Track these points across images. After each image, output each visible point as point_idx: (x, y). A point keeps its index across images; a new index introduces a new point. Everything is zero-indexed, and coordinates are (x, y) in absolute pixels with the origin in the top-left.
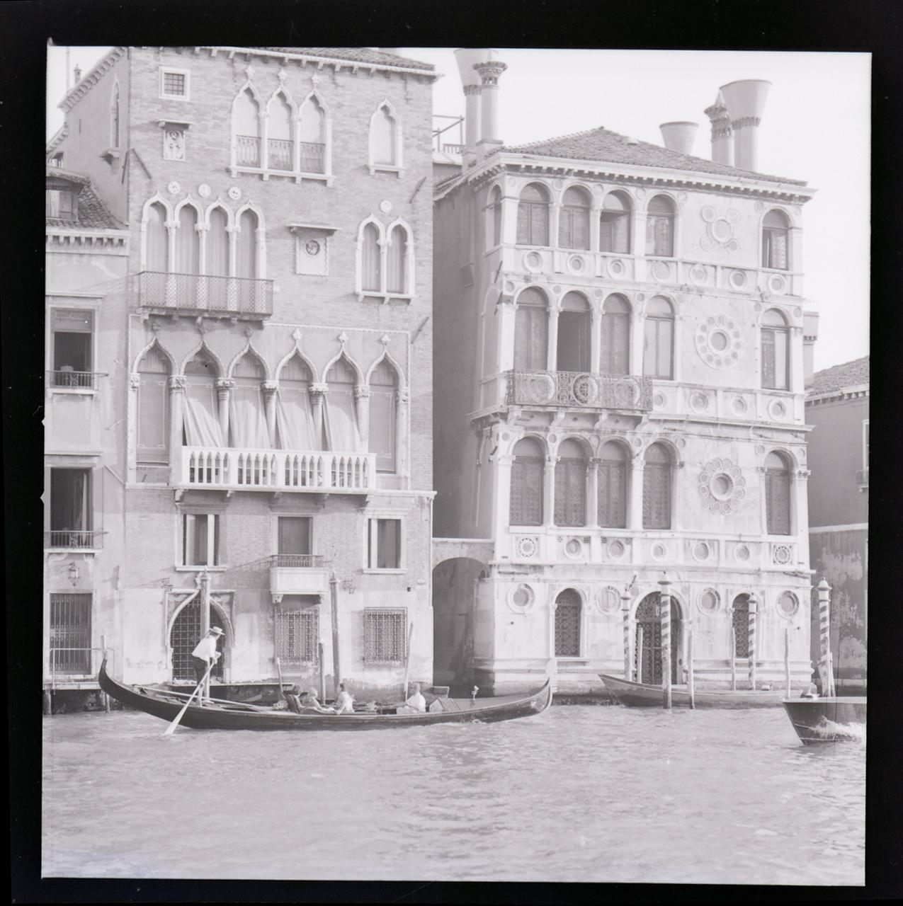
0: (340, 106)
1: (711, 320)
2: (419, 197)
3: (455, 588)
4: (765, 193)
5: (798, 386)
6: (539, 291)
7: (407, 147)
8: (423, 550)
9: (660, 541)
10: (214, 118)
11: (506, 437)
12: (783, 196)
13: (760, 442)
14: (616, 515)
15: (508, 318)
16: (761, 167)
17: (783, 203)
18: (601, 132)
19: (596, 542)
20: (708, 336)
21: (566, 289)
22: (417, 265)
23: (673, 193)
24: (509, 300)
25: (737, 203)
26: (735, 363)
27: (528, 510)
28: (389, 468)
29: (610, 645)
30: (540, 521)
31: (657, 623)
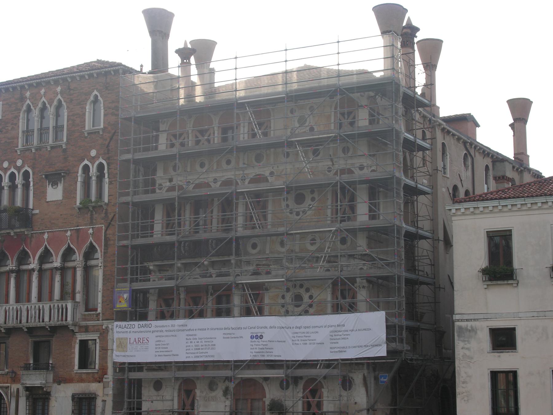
0: (71, 100)
7: (105, 115)
10: (12, 124)
22: (109, 184)
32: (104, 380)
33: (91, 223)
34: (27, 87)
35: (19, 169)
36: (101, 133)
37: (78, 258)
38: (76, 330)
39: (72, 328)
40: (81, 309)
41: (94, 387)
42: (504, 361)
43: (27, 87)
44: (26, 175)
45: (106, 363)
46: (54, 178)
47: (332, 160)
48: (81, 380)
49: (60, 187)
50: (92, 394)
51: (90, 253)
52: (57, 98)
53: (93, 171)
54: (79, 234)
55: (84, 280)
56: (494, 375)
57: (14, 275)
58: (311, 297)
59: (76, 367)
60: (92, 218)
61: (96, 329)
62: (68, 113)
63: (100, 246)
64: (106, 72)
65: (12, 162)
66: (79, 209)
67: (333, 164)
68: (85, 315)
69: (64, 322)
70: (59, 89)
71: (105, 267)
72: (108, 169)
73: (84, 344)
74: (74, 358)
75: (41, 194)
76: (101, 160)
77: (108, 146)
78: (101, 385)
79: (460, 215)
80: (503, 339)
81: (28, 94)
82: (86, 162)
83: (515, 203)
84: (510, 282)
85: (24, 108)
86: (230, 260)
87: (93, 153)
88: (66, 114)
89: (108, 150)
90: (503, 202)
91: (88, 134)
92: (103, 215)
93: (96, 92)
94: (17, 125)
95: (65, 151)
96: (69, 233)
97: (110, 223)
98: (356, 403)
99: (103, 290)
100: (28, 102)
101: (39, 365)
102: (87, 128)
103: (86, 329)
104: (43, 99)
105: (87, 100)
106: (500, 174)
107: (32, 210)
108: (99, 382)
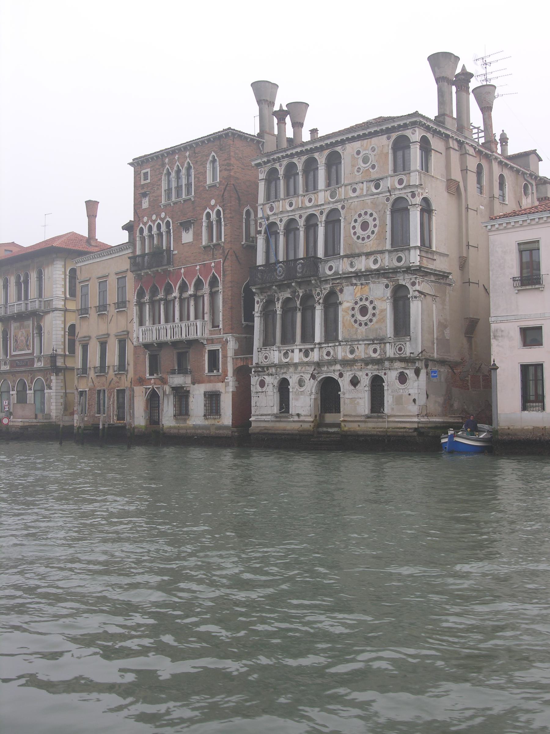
0: (197, 162)
1: (360, 215)
2: (225, 194)
4: (387, 129)
7: (220, 171)
9: (327, 348)
11: (258, 302)
12: (399, 126)
13: (385, 281)
14: (308, 335)
17: (403, 130)
19: (297, 351)
20: (358, 226)
21: (285, 220)
23: (339, 149)
25: (375, 141)
26: (372, 236)
32: (226, 381)
33: (213, 258)
34: (166, 155)
35: (163, 220)
36: (218, 186)
37: (206, 287)
38: (205, 342)
39: (202, 341)
40: (209, 326)
41: (219, 387)
42: (532, 356)
43: (166, 155)
44: (168, 224)
45: (227, 367)
46: (186, 226)
47: (389, 191)
48: (210, 382)
49: (191, 232)
50: (217, 391)
51: (214, 282)
52: (187, 161)
53: (213, 216)
55: (210, 303)
57: (162, 302)
58: (374, 308)
59: (207, 371)
60: (213, 254)
61: (219, 341)
62: (195, 172)
63: (220, 276)
64: (219, 136)
65: (158, 215)
66: (205, 247)
67: (391, 195)
68: (211, 331)
69: (195, 336)
70: (188, 154)
71: (223, 292)
72: (224, 213)
73: (213, 355)
74: (205, 364)
75: (178, 238)
76: (218, 207)
77: (223, 196)
78: (224, 384)
79: (494, 231)
80: (531, 336)
82: (208, 210)
83: (541, 216)
84: (537, 286)
85: (165, 172)
86: (311, 281)
87: (213, 202)
88: (193, 173)
89: (223, 199)
90: (531, 217)
91: (209, 187)
92: (221, 251)
93: (213, 153)
95: (193, 202)
96: (198, 267)
97: (226, 257)
98: (409, 394)
99: (223, 310)
100: (167, 166)
101: (182, 370)
102: (208, 183)
103: (211, 341)
104: (178, 163)
105: (207, 160)
106: (543, 196)
107: (173, 251)
108: (223, 382)
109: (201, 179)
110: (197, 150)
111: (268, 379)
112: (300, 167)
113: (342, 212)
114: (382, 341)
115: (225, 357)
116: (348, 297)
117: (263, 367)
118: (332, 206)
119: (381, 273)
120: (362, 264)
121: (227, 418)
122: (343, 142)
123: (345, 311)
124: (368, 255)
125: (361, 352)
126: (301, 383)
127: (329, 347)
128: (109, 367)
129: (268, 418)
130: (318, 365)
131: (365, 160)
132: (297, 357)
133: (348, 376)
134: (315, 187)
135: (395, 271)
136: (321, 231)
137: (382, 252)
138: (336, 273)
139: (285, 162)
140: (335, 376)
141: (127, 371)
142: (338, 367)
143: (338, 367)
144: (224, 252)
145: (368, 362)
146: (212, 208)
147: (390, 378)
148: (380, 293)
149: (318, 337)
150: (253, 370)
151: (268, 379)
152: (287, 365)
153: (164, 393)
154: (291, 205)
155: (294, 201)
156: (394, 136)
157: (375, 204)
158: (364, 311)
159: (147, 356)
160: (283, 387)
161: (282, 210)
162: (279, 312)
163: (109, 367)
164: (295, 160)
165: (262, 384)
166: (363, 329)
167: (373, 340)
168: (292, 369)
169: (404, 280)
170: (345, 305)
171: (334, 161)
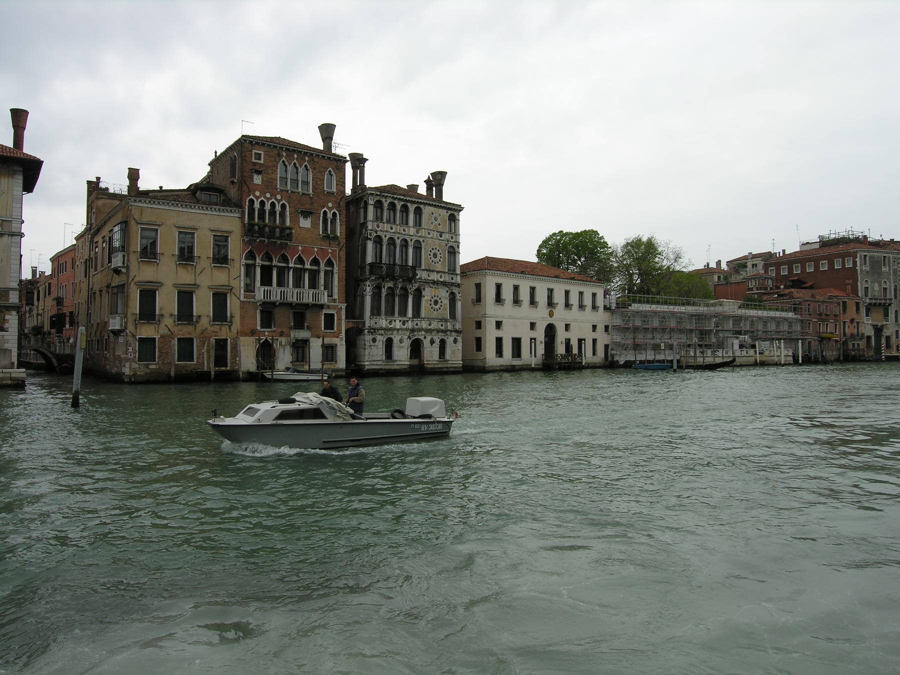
3: (353, 339)
5: (458, 271)
6: (379, 237)
8: (342, 324)
14: (403, 313)
15: (370, 246)
16: (445, 199)
18: (393, 185)
19: (398, 321)
21: (388, 237)
23: (422, 206)
24: (370, 239)
25: (441, 210)
27: (376, 312)
28: (330, 295)
29: (402, 356)
30: (379, 314)
31: (416, 348)
35: (279, 201)
41: (335, 341)
42: (499, 334)
44: (283, 206)
46: (306, 214)
51: (330, 263)
53: (330, 215)
54: (323, 252)
56: (497, 338)
61: (335, 307)
65: (273, 195)
75: (295, 221)
81: (284, 154)
94: (276, 171)
103: (329, 307)
109: (319, 182)
110: (315, 159)
111: (379, 338)
112: (398, 207)
113: (423, 244)
114: (446, 321)
115: (340, 319)
116: (428, 293)
117: (374, 329)
118: (417, 238)
119: (444, 284)
120: (434, 277)
121: (341, 363)
122: (425, 204)
123: (427, 301)
124: (438, 272)
125: (435, 325)
126: (401, 341)
127: (416, 321)
128: (199, 317)
129: (380, 363)
130: (413, 330)
131: (436, 219)
132: (398, 325)
133: (429, 338)
134: (407, 223)
135: (452, 284)
136: (411, 251)
137: (445, 273)
138: (420, 278)
139: (389, 200)
140: (422, 338)
141: (231, 322)
142: (423, 333)
143: (423, 333)
144: (339, 244)
145: (438, 331)
146: (330, 209)
147: (450, 340)
148: (443, 294)
149: (410, 313)
150: (366, 331)
151: (379, 338)
152: (391, 329)
153: (281, 344)
154: (392, 228)
155: (394, 227)
156: (450, 212)
157: (440, 245)
158: (436, 303)
159: (258, 311)
160: (389, 343)
161: (386, 230)
162: (383, 295)
163: (199, 317)
164: (396, 202)
165: (374, 340)
166: (435, 312)
167: (442, 320)
168: (395, 332)
169: (456, 290)
170: (426, 298)
171: (418, 211)
